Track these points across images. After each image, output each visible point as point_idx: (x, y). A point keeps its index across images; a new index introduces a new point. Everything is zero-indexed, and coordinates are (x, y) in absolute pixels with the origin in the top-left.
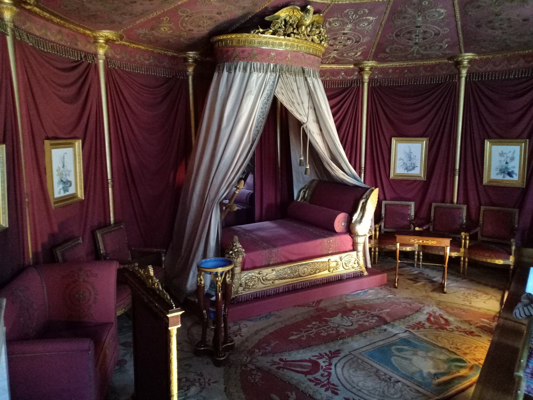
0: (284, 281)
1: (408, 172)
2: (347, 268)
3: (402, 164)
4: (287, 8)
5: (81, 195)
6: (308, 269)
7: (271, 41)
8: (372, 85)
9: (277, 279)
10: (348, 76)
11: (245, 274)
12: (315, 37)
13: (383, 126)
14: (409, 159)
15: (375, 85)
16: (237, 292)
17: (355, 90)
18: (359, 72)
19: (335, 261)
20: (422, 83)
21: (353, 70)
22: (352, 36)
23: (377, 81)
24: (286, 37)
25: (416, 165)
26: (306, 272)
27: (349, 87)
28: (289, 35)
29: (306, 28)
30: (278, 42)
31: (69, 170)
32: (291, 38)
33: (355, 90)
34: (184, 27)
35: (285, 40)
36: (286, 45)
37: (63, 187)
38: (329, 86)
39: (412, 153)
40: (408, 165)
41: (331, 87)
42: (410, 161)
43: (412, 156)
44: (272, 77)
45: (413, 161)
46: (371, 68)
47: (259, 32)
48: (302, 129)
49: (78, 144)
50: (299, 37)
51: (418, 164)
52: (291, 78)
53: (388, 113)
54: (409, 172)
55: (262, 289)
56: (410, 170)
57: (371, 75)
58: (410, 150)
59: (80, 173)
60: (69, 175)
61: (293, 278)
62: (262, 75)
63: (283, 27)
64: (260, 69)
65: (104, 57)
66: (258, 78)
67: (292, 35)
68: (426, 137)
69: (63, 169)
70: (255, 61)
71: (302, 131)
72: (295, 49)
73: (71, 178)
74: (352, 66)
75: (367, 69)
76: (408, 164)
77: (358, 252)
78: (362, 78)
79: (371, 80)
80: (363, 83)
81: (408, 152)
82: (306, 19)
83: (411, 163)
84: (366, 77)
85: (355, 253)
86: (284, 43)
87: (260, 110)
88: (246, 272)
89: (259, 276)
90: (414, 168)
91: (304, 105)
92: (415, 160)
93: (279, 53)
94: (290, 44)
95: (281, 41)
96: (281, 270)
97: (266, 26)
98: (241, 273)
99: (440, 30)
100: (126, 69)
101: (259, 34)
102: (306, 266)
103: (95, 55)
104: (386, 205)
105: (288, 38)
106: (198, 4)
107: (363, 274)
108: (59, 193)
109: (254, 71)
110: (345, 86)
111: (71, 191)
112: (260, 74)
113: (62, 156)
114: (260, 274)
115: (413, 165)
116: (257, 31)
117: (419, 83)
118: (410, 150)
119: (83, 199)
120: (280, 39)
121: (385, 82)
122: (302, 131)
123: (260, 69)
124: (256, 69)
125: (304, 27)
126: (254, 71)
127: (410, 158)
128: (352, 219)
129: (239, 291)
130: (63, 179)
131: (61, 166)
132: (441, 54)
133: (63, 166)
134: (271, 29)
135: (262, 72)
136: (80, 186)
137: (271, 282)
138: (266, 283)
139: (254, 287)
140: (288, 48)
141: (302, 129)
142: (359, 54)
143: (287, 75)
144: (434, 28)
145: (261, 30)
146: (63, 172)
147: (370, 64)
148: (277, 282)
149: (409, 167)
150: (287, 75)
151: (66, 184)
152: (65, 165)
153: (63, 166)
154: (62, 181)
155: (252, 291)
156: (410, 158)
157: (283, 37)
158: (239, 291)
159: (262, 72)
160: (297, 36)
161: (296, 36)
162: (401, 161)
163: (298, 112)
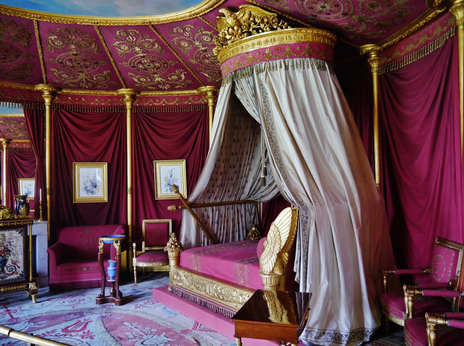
31: (177, 178)
69: (170, 178)
113: (171, 170)
130: (170, 184)
131: (169, 176)
133: (171, 176)
146: (171, 180)
153: (171, 176)
154: (169, 184)
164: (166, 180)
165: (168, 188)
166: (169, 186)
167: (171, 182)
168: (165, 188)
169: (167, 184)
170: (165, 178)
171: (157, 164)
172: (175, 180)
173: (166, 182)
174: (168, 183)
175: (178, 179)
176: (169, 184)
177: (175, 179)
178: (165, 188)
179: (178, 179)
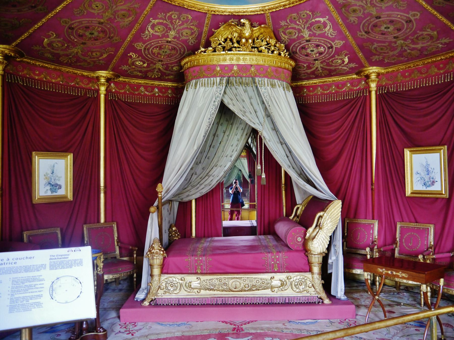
0: (212, 292)
1: (426, 188)
2: (298, 290)
3: (419, 179)
4: (223, 26)
5: (70, 197)
6: (240, 284)
7: (215, 58)
8: (379, 92)
9: (202, 289)
10: (355, 86)
11: (166, 277)
12: (263, 48)
13: (394, 135)
14: (426, 173)
15: (382, 92)
16: (156, 294)
17: (361, 101)
18: (365, 81)
19: (280, 280)
20: (435, 82)
21: (359, 81)
22: (318, 42)
23: (385, 88)
24: (227, 52)
25: (436, 180)
26: (237, 287)
27: (356, 97)
28: (230, 50)
29: (247, 40)
30: (221, 57)
31: (59, 176)
32: (232, 52)
33: (361, 101)
34: (152, 59)
35: (227, 54)
36: (231, 59)
37: (51, 189)
38: (334, 99)
39: (429, 165)
40: (427, 180)
41: (337, 99)
42: (428, 174)
43: (430, 169)
44: (219, 89)
45: (432, 175)
46: (378, 75)
47: (202, 51)
48: (258, 137)
49: (70, 157)
50: (241, 50)
51: (438, 178)
52: (241, 89)
53: (399, 122)
54: (429, 189)
55: (185, 297)
56: (429, 186)
57: (378, 82)
58: (427, 162)
59: (70, 179)
60: (59, 180)
61: (223, 291)
62: (209, 89)
63: (223, 43)
64: (208, 84)
65: (105, 92)
66: (205, 92)
67: (234, 49)
68: (443, 145)
69: (52, 175)
70: (203, 78)
71: (258, 139)
72: (241, 63)
73: (62, 182)
74: (355, 76)
75: (373, 77)
76: (426, 179)
77: (313, 273)
78: (369, 87)
79: (379, 87)
80: (370, 92)
81: (425, 164)
82: (243, 32)
83: (430, 177)
84: (373, 86)
85: (308, 275)
86: (228, 57)
87: (208, 120)
88: (166, 276)
89: (181, 282)
90: (433, 183)
91: (257, 113)
92: (433, 174)
93: (223, 67)
94: (235, 58)
95: (225, 56)
96: (207, 280)
97: (208, 44)
98: (160, 275)
99: (407, 15)
100: (128, 100)
101: (202, 53)
102: (238, 280)
103: (98, 91)
104: (401, 227)
105: (229, 52)
106: (144, 37)
107: (322, 302)
108: (46, 192)
109: (202, 85)
110: (351, 97)
111: (61, 192)
112: (208, 88)
113: (52, 165)
114: (182, 280)
115: (431, 180)
116: (200, 51)
117: (432, 83)
118: (427, 162)
119: (72, 200)
120: (223, 54)
121: (394, 89)
122: (258, 139)
123: (208, 84)
124: (203, 84)
125: (244, 40)
126: (202, 85)
127: (428, 172)
128: (305, 234)
129: (158, 294)
130: (51, 182)
131: (49, 172)
132: (441, 46)
133: (53, 173)
134: (212, 47)
135: (209, 86)
136: (70, 189)
137: (196, 290)
138: (189, 291)
139: (175, 292)
140: (232, 62)
141: (258, 137)
142: (346, 60)
143: (237, 87)
144: (398, 15)
145: (203, 49)
146: (52, 178)
147: (377, 71)
148: (203, 292)
149: (428, 182)
150: (237, 87)
151: (55, 186)
152: (55, 172)
153: (53, 173)
154: (50, 183)
155: (173, 296)
156: (428, 172)
157: (224, 52)
158: (158, 294)
159: (209, 86)
160: (239, 49)
161: (237, 49)
162: (418, 175)
163: (251, 121)
164: (46, 178)
165: (48, 187)
166: (49, 185)
167: (53, 180)
168: (44, 188)
169: (48, 183)
170: (45, 175)
171: (36, 157)
172: (57, 178)
173: (46, 180)
174: (48, 182)
175: (61, 177)
176: (50, 183)
177: (57, 176)
178: (44, 188)
179: (61, 177)
